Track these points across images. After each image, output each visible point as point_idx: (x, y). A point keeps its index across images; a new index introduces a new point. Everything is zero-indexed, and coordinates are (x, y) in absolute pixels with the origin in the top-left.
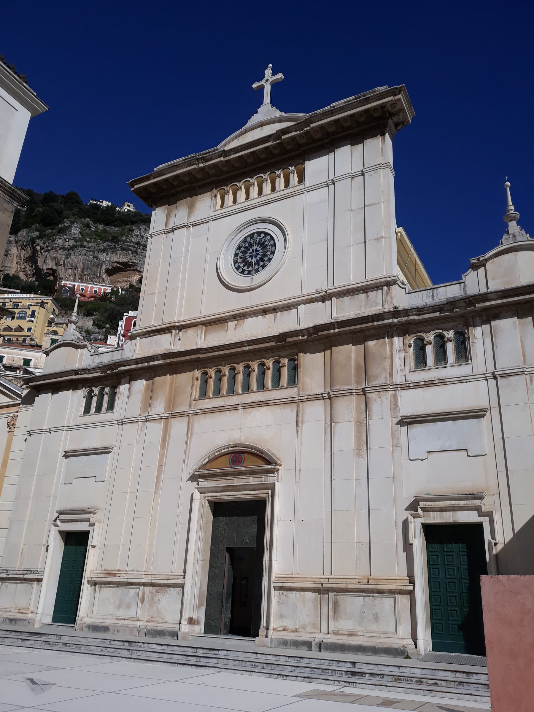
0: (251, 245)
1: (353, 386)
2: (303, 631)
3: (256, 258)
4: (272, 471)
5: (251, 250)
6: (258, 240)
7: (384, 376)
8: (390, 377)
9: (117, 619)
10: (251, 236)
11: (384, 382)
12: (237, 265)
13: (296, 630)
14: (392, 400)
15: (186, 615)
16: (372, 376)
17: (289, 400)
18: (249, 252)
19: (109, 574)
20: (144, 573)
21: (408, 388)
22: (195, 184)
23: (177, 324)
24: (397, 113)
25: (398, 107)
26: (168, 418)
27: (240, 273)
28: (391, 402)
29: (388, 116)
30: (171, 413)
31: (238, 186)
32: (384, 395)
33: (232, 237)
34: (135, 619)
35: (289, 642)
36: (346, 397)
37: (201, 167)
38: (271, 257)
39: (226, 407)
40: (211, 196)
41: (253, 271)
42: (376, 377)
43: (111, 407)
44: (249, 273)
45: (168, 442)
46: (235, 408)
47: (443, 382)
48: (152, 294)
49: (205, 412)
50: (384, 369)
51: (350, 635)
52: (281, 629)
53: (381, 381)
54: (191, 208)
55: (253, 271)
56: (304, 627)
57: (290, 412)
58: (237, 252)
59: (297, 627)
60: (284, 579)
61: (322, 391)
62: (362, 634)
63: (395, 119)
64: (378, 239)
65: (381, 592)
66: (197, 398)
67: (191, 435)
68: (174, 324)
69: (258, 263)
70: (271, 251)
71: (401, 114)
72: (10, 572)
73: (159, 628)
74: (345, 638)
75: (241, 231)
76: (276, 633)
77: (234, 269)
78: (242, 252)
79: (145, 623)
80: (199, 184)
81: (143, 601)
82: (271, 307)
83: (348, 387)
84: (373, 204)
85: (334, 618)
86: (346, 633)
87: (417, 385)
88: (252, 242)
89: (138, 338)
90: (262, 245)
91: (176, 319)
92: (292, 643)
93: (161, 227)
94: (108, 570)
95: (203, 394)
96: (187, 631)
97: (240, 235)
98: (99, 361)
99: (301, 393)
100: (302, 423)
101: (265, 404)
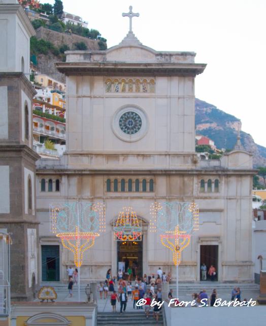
10: (128, 113)
21: (198, 198)
43: (58, 189)
44: (128, 133)
46: (127, 198)
47: (210, 198)
49: (112, 198)
53: (188, 195)
61: (165, 195)
65: (186, 266)
81: (92, 271)
87: (201, 198)
89: (69, 156)
95: (109, 190)
97: (122, 111)
101: (141, 198)
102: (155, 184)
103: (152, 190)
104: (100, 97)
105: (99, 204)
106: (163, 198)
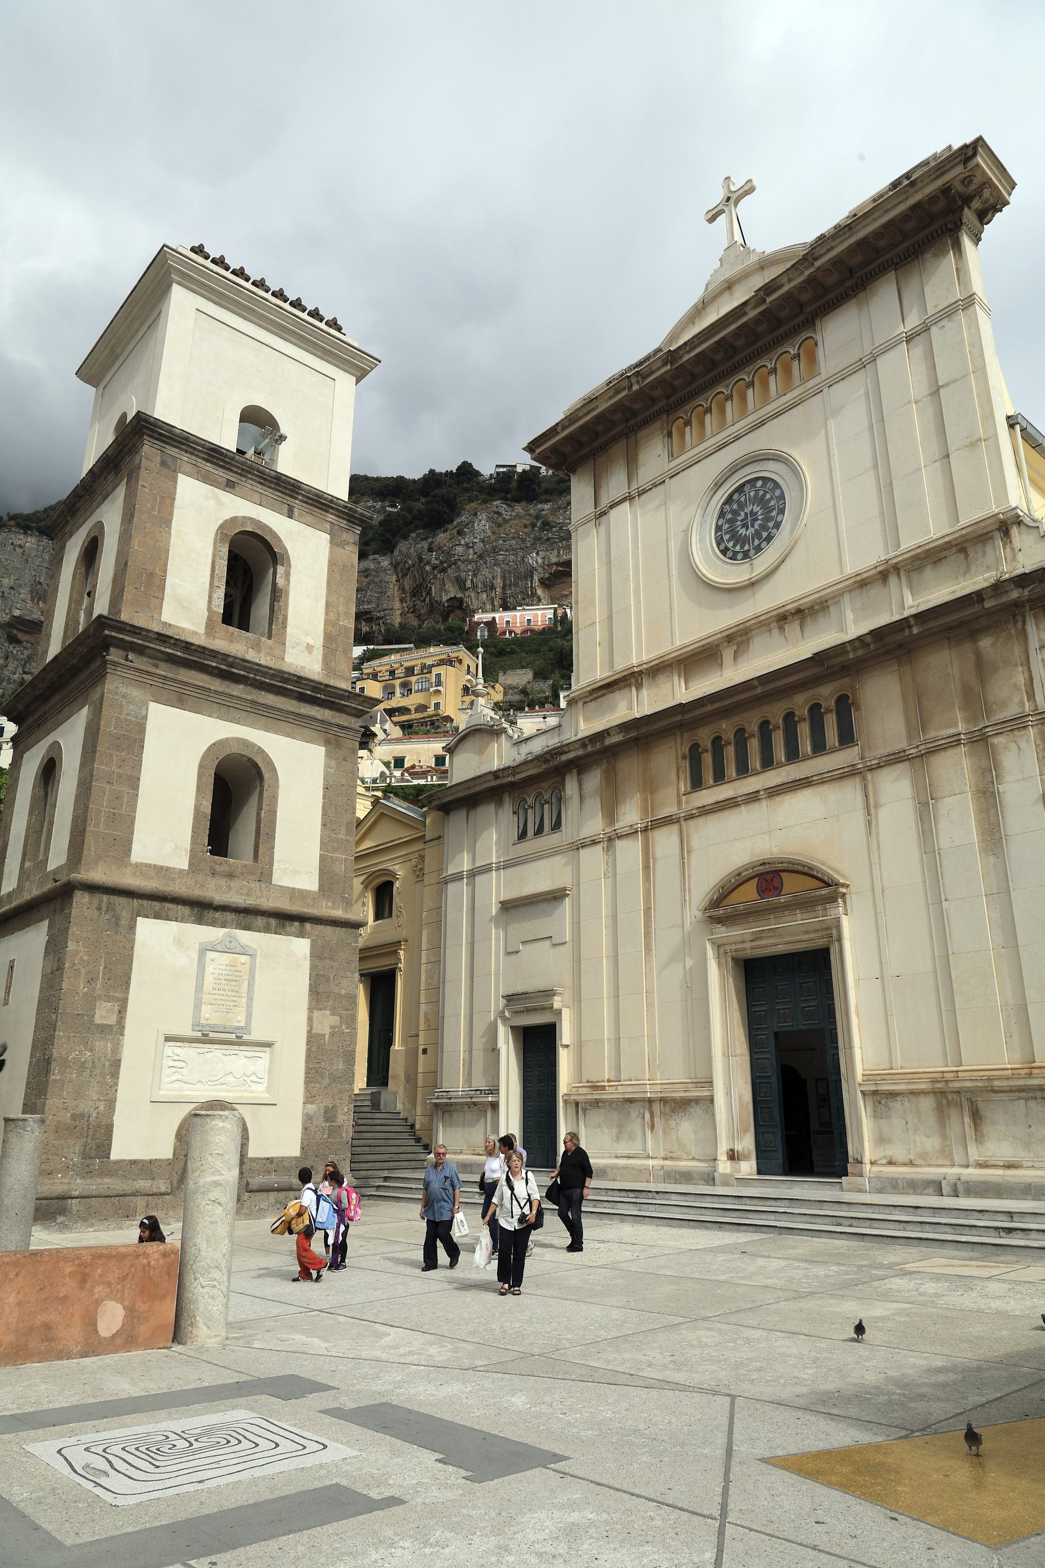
0: (742, 506)
1: (961, 727)
2: (924, 1163)
3: (753, 526)
4: (832, 899)
5: (742, 514)
6: (752, 494)
7: (1016, 700)
8: (1028, 701)
9: (617, 1157)
10: (740, 489)
11: (1019, 710)
13: (911, 1164)
14: (1038, 742)
15: (723, 1148)
16: (993, 703)
17: (846, 770)
18: (740, 518)
19: (595, 1088)
20: (648, 1082)
22: (633, 421)
23: (636, 669)
24: (979, 192)
25: (977, 180)
26: (645, 830)
27: (730, 558)
28: (1037, 746)
29: (960, 203)
31: (705, 406)
32: (1021, 736)
33: (708, 499)
34: (643, 1156)
35: (900, 1183)
36: (949, 749)
37: (637, 390)
38: (779, 519)
39: (739, 799)
40: (661, 436)
41: (752, 552)
42: (1003, 705)
44: (746, 555)
45: (654, 869)
46: (753, 798)
48: (590, 625)
49: (706, 811)
50: (1016, 687)
51: (1009, 1166)
52: (884, 1161)
53: (1011, 711)
54: (632, 464)
55: (752, 552)
56: (924, 1155)
57: (850, 793)
58: (720, 523)
59: (912, 1157)
60: (878, 1078)
61: (903, 745)
62: (1030, 1164)
63: (976, 204)
64: (973, 445)
66: (689, 789)
67: (688, 852)
68: (632, 671)
69: (758, 534)
70: (778, 508)
71: (986, 193)
73: (683, 1169)
74: (1000, 1172)
75: (720, 486)
76: (875, 1169)
79: (661, 1162)
80: (639, 419)
82: (792, 609)
83: (952, 731)
84: (953, 382)
85: (976, 1140)
86: (1001, 1164)
88: (743, 499)
90: (761, 501)
91: (635, 661)
92: (905, 1184)
93: (590, 509)
94: (592, 1082)
96: (728, 1171)
97: (721, 492)
98: (527, 751)
99: (867, 754)
100: (876, 807)
101: (805, 783)
102: (858, 709)
103: (847, 738)
104: (655, 486)
105: (666, 841)
106: (896, 758)
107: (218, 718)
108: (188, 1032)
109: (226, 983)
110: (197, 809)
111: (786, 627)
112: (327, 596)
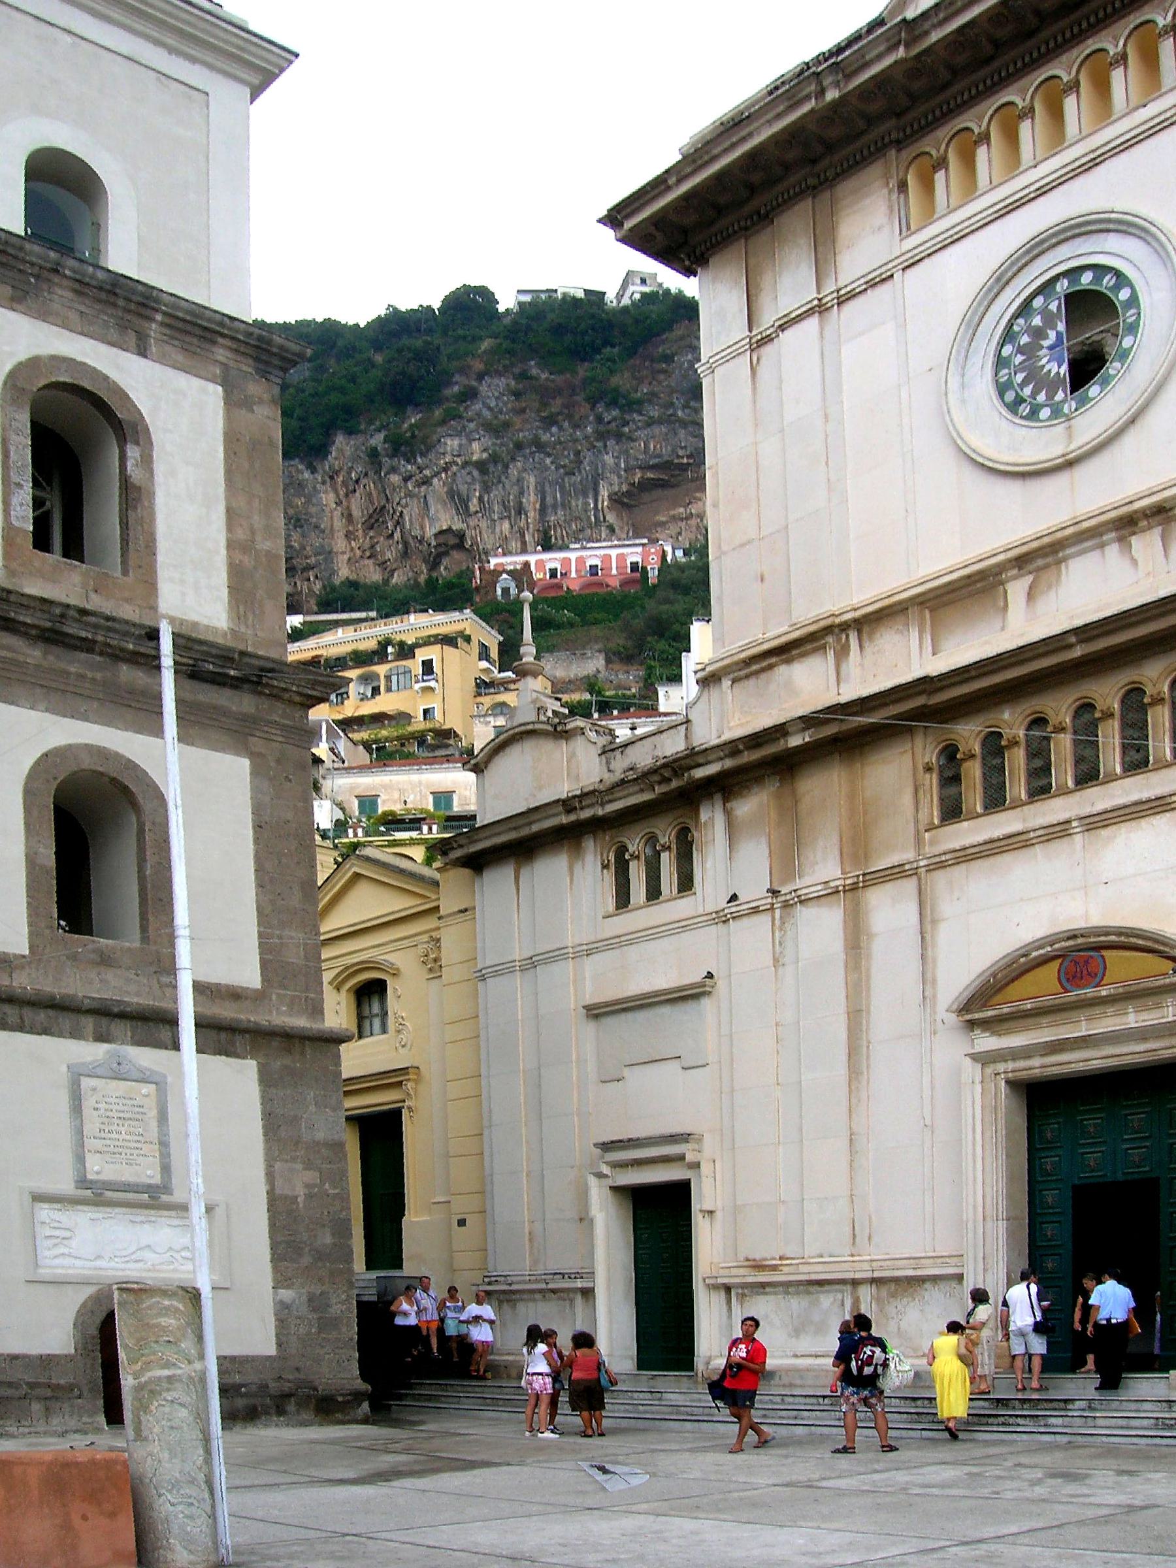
12: (1010, 396)
30: (864, 875)
72: (514, 1279)
77: (1004, 411)
78: (1020, 350)
107: (47, 710)
108: (66, 1185)
109: (121, 1122)
110: (31, 861)
111: (1134, 540)
112: (227, 499)
